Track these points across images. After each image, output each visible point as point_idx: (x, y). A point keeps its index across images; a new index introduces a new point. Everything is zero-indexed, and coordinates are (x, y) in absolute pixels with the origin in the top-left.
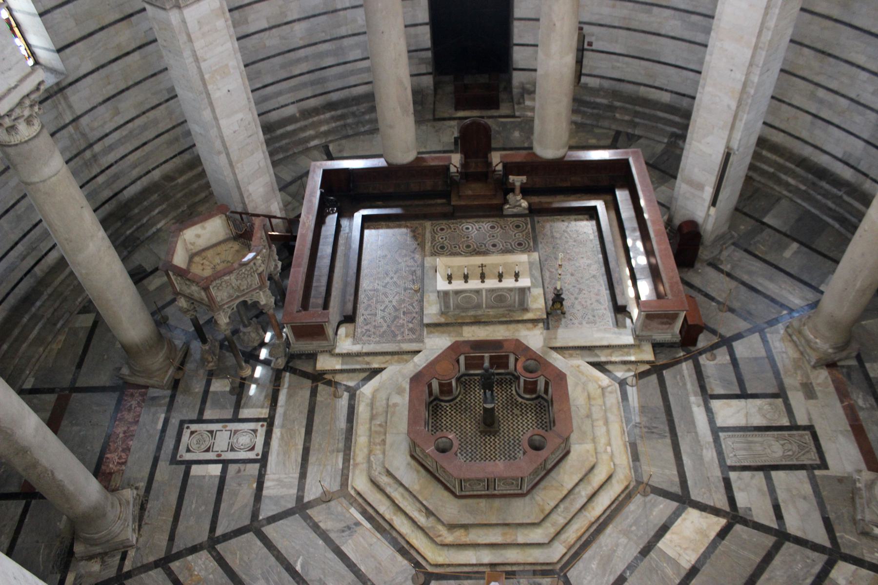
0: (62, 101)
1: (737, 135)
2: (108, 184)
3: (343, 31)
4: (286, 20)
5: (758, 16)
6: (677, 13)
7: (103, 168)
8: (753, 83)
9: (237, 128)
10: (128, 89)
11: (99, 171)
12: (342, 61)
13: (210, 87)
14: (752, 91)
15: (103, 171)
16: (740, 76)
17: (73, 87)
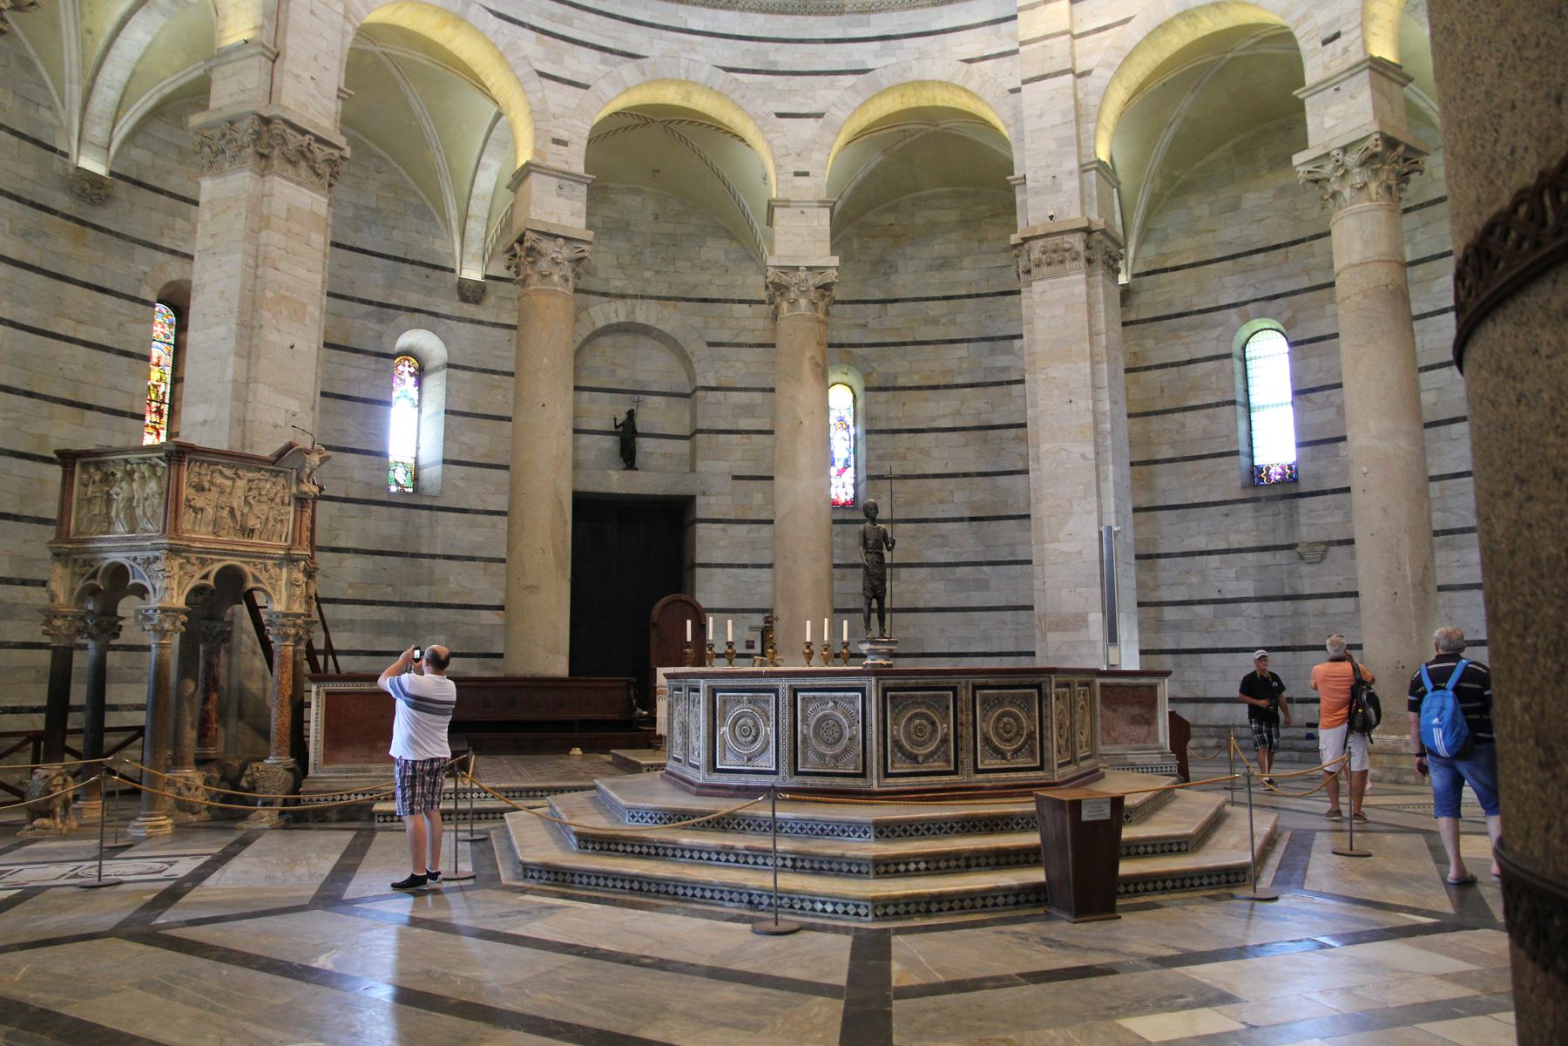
1: (1110, 504)
3: (422, 594)
4: (334, 544)
5: (1081, 316)
6: (935, 570)
8: (1104, 413)
9: (281, 423)
10: (17, 518)
13: (266, 314)
14: (1108, 426)
16: (1084, 404)
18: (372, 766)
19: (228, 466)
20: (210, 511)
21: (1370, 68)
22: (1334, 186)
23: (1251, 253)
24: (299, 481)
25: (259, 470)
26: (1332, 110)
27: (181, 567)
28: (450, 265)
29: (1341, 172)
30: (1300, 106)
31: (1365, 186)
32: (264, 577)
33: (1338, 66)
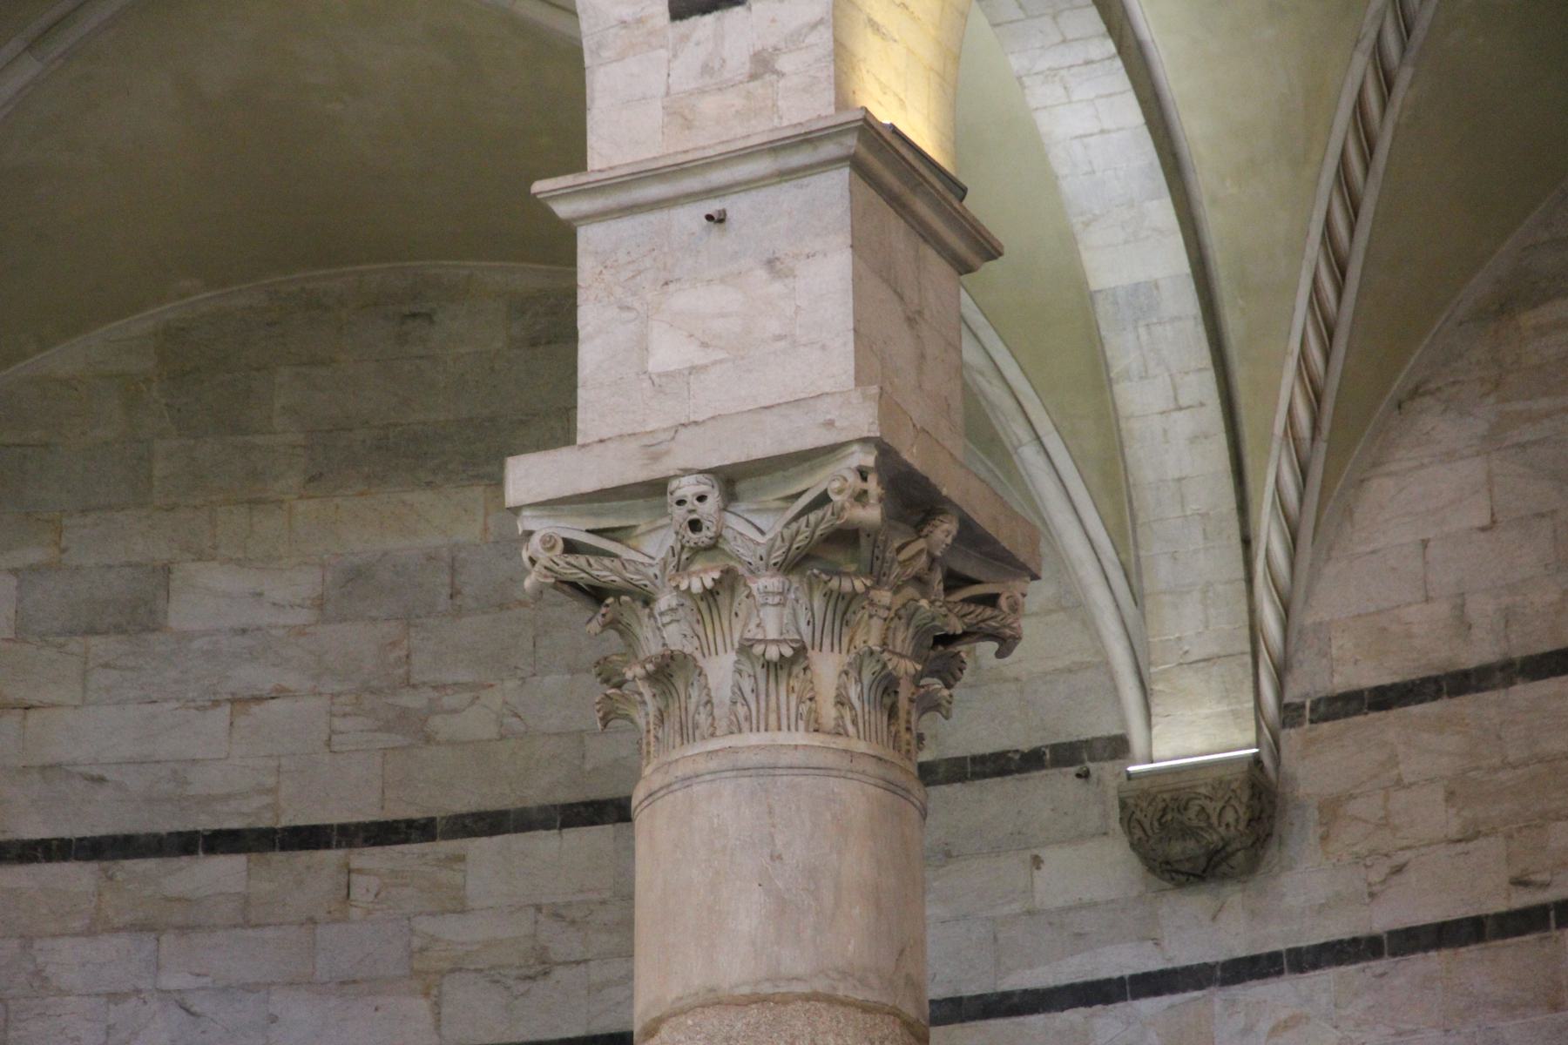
21: (856, 165)
22: (668, 631)
23: (187, 844)
26: (683, 300)
29: (703, 577)
30: (558, 245)
31: (789, 664)
33: (724, 121)
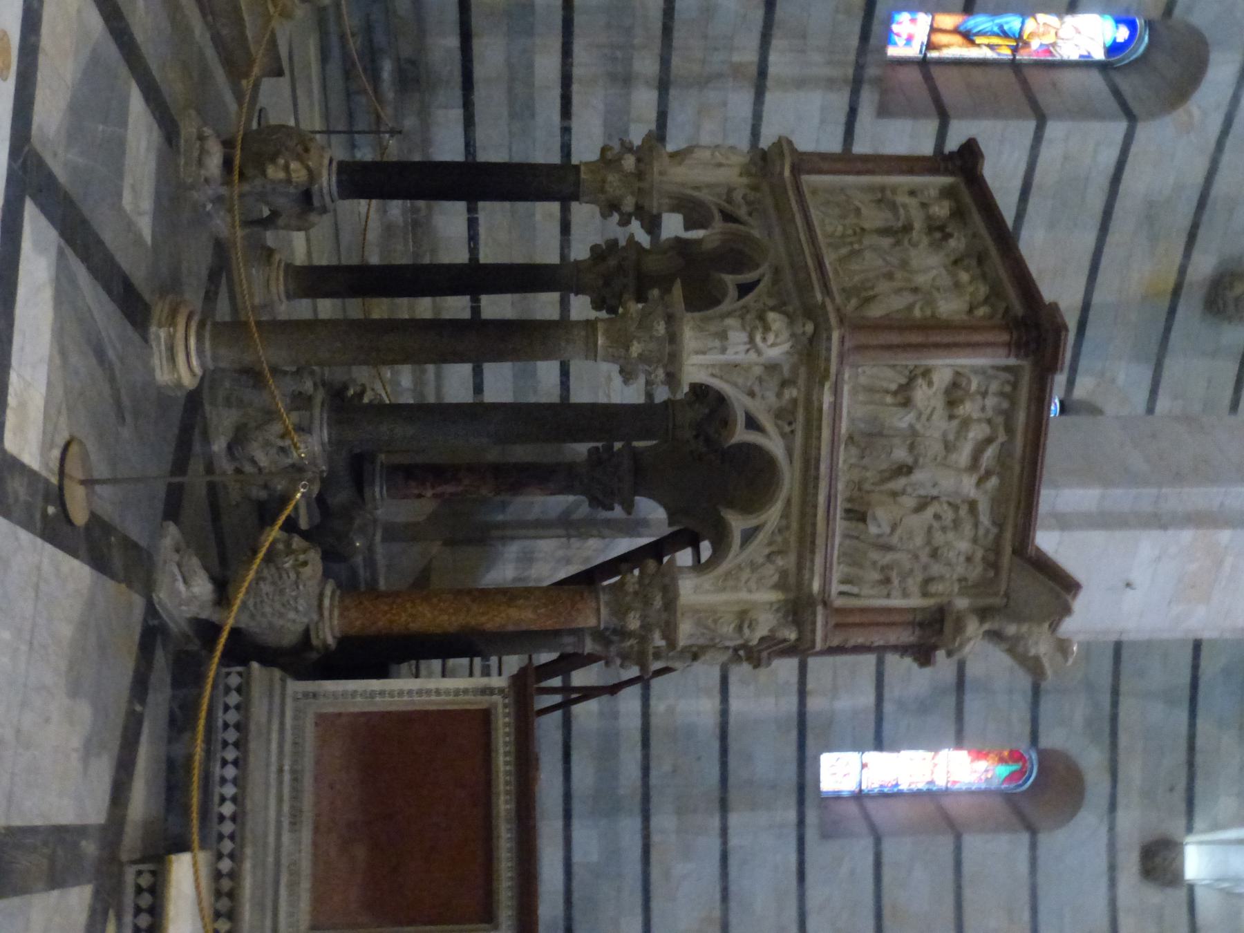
0: (828, 71)
2: (518, 76)
3: (663, 821)
7: (575, 87)
11: (577, 72)
12: (577, 806)
13: (1187, 535)
15: (566, 80)
17: (842, 118)
18: (306, 835)
19: (1003, 458)
20: (902, 420)
24: (984, 613)
25: (999, 524)
27: (772, 368)
28: (1199, 823)
32: (757, 549)
